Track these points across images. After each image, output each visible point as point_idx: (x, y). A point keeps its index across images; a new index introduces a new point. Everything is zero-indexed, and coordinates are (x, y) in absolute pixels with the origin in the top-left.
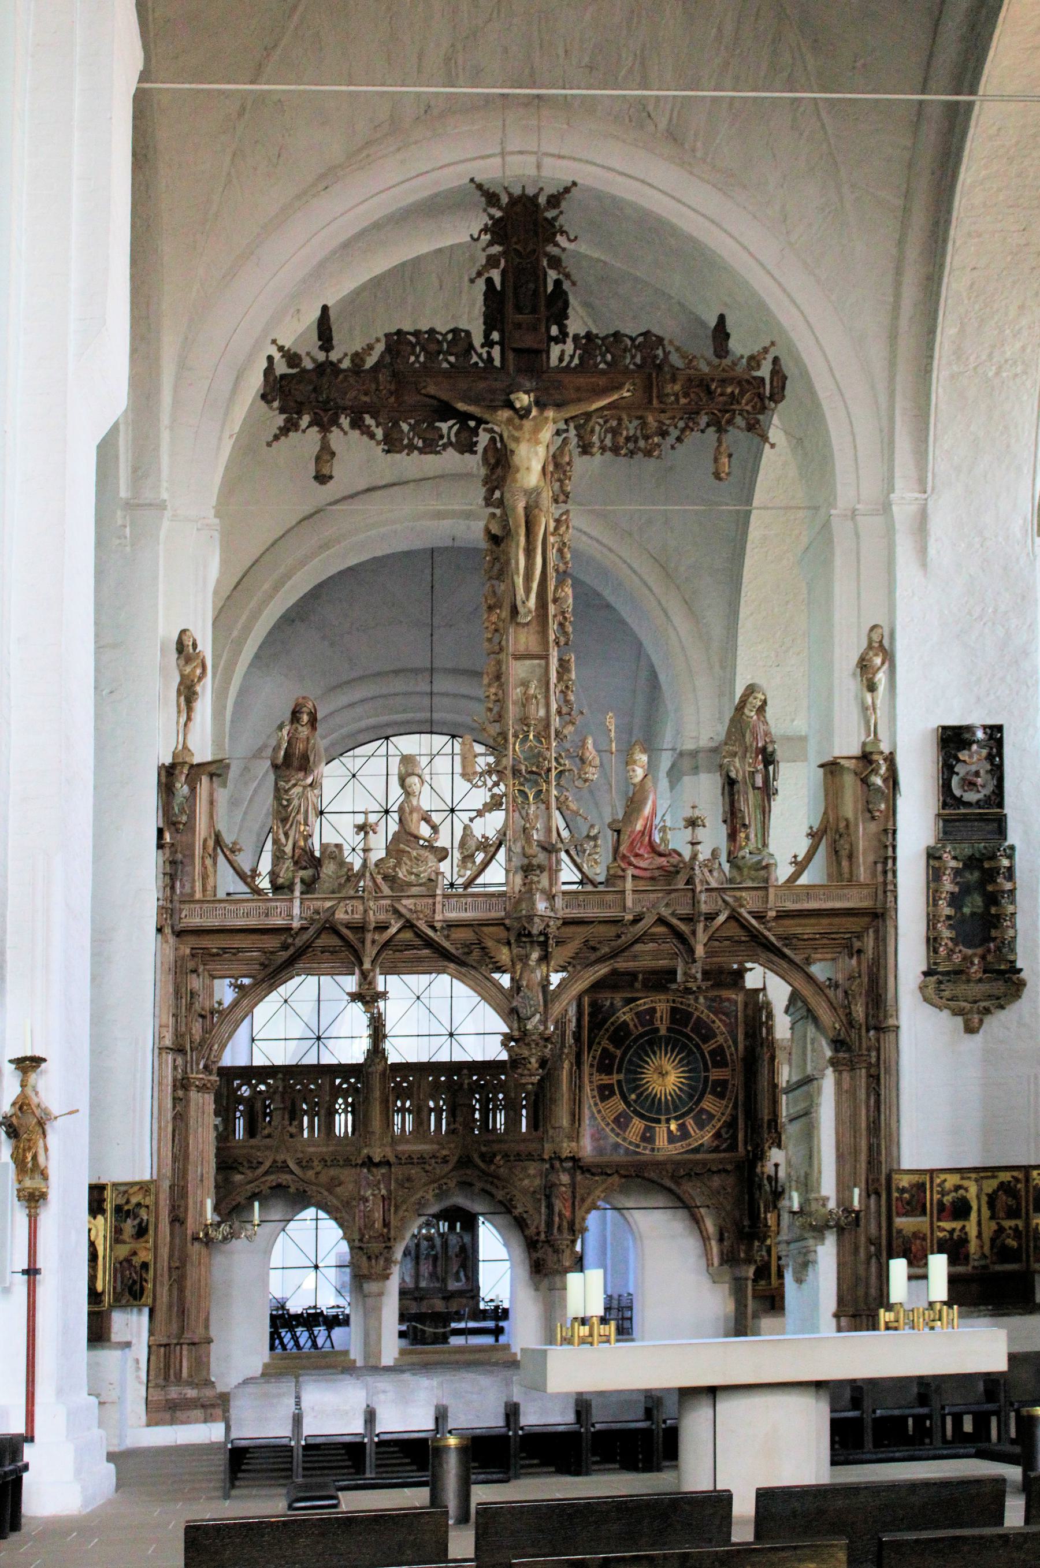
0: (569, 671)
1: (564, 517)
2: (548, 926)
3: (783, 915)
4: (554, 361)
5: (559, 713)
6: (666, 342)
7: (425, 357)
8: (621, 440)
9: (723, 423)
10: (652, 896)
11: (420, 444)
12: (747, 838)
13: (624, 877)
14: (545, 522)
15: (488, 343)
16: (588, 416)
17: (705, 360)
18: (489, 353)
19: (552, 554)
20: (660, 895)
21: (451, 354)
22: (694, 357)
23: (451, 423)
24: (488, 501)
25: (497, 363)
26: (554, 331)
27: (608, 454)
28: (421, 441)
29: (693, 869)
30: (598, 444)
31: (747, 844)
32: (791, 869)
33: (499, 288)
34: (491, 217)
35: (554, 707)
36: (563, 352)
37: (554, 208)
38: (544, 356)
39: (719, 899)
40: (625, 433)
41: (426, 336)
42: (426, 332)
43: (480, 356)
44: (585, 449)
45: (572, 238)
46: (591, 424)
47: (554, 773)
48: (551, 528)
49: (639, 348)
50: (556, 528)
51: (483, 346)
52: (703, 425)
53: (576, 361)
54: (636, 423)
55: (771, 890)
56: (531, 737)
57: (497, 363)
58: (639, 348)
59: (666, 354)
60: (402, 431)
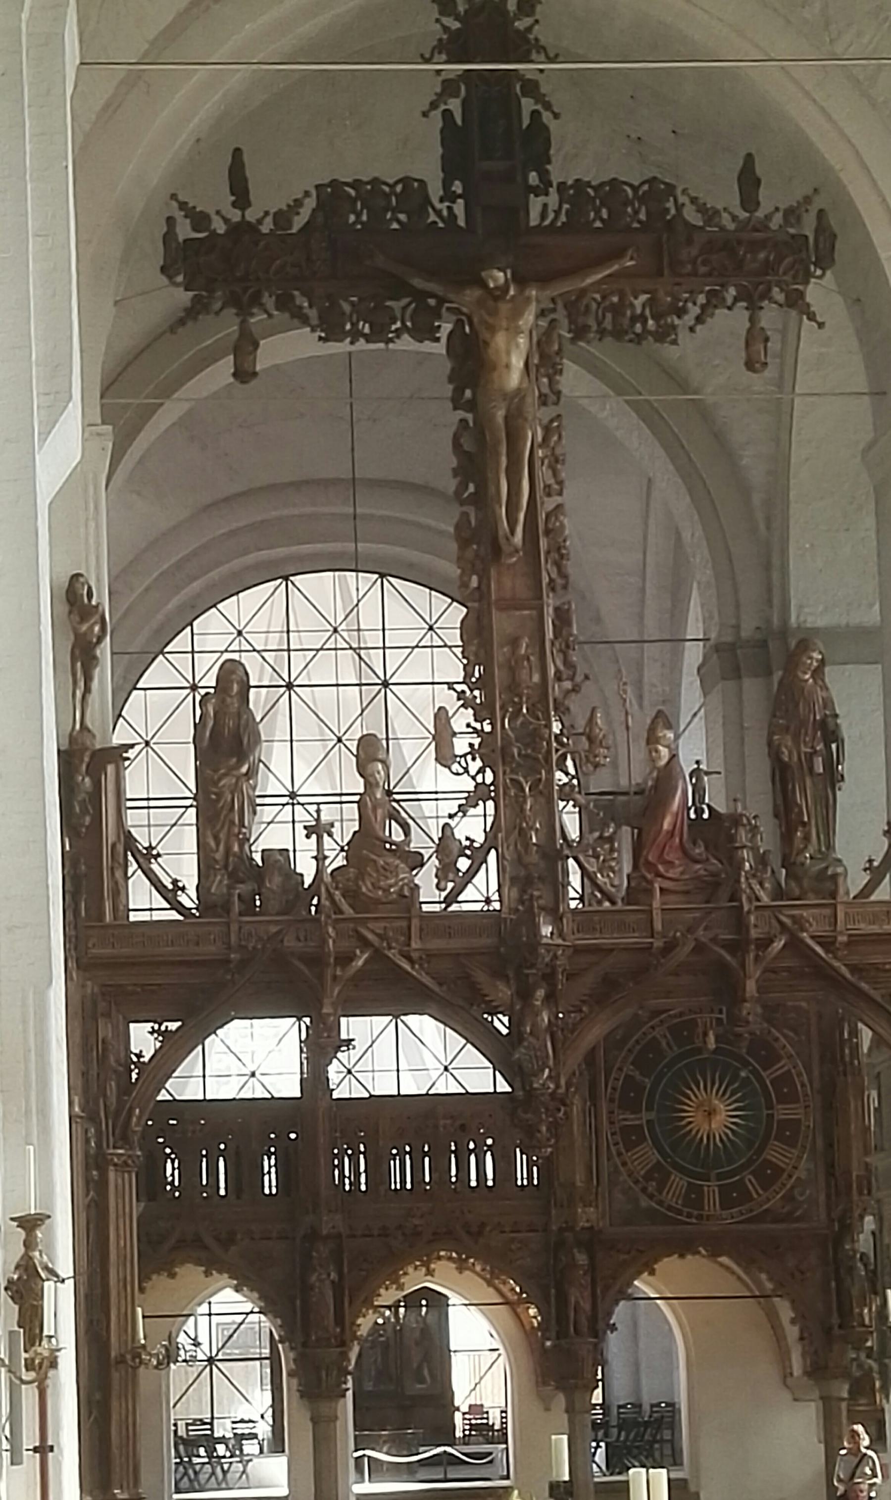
0: (570, 624)
1: (555, 424)
2: (555, 957)
3: (856, 941)
4: (534, 221)
5: (559, 678)
6: (679, 191)
7: (368, 217)
8: (626, 322)
9: (756, 297)
10: (689, 916)
11: (367, 330)
12: (807, 838)
13: (650, 892)
14: (532, 434)
15: (449, 196)
16: (582, 293)
17: (730, 213)
18: (449, 208)
19: (544, 474)
20: (697, 915)
21: (401, 212)
22: (717, 212)
23: (406, 301)
24: (457, 402)
25: (461, 222)
26: (533, 178)
27: (608, 340)
28: (367, 325)
29: (738, 881)
30: (595, 327)
31: (806, 847)
32: (866, 878)
33: (459, 121)
34: (446, 29)
35: (552, 671)
36: (545, 206)
37: (528, 16)
38: (522, 214)
39: (774, 922)
40: (629, 313)
41: (369, 187)
42: (368, 183)
43: (438, 213)
44: (580, 332)
45: (552, 55)
46: (585, 302)
47: (555, 757)
48: (540, 439)
49: (642, 200)
50: (545, 439)
51: (442, 200)
52: (729, 301)
53: (563, 218)
54: (644, 297)
55: (840, 908)
56: (525, 711)
57: (461, 222)
58: (642, 200)
59: (679, 207)
60: (344, 314)
